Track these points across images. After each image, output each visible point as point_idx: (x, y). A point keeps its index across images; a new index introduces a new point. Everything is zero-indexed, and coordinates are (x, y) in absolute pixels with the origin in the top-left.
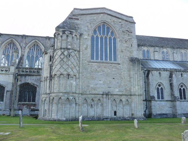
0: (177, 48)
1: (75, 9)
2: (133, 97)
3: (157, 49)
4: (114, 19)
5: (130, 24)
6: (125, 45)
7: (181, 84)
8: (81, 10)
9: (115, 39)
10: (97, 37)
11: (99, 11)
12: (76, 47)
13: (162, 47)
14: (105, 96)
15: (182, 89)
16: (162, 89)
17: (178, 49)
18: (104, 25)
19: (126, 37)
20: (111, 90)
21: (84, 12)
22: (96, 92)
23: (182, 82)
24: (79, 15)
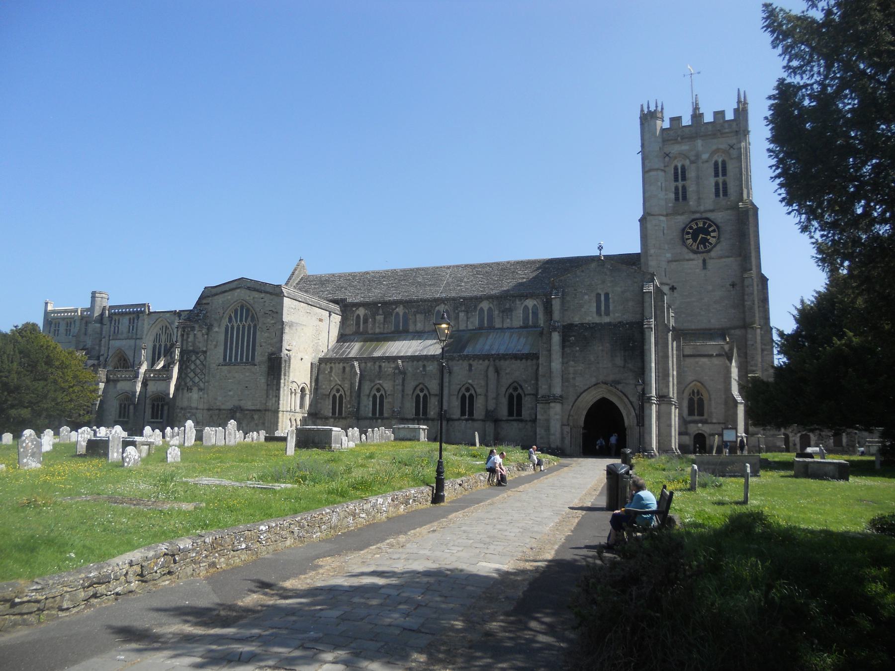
1: (206, 288)
4: (256, 295)
7: (421, 386)
9: (255, 326)
18: (242, 307)
19: (270, 321)
20: (242, 403)
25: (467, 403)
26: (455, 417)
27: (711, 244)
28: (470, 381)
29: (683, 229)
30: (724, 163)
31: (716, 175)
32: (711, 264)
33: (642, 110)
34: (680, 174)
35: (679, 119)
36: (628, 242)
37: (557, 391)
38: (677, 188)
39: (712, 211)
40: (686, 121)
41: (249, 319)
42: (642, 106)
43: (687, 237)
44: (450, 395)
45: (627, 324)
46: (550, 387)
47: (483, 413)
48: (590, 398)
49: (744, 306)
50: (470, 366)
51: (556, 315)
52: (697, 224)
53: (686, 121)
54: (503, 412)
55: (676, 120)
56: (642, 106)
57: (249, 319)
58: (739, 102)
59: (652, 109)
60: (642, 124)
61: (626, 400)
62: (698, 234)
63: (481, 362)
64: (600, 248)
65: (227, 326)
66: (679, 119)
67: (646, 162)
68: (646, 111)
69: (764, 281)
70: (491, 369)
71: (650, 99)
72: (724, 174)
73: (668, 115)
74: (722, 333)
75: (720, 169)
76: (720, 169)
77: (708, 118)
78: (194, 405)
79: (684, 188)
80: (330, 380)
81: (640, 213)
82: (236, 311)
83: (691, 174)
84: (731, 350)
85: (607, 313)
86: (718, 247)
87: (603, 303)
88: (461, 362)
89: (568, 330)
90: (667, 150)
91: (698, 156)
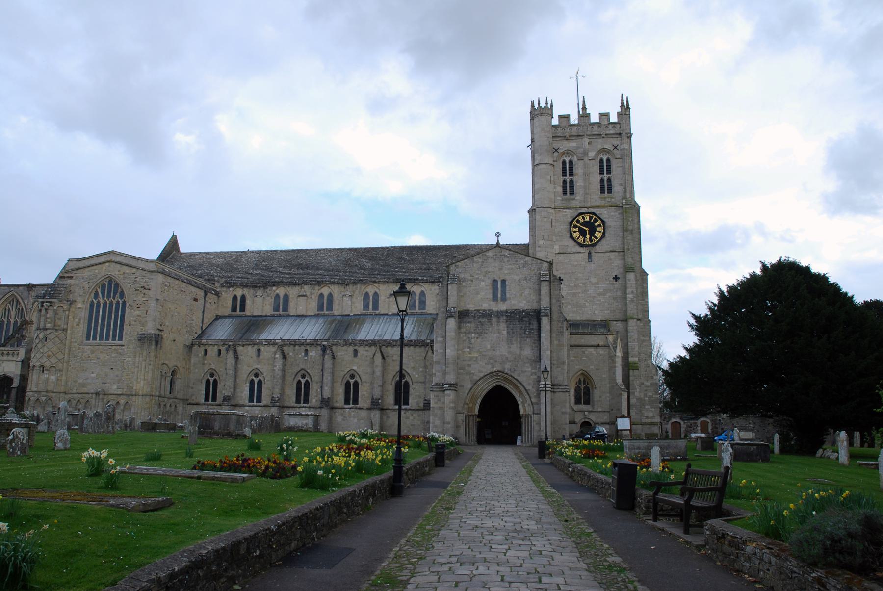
0: (355, 283)
1: (70, 260)
2: (134, 398)
3: (307, 289)
4: (127, 270)
5: (149, 275)
6: (137, 313)
7: (303, 372)
8: (78, 260)
9: (124, 303)
10: (99, 302)
11: (102, 259)
12: (61, 324)
13: (319, 283)
14: (94, 396)
15: (303, 381)
16: (260, 382)
17: (359, 286)
18: (110, 282)
19: (140, 299)
21: (81, 264)
22: (86, 390)
23: (302, 366)
24: (73, 270)
25: (352, 392)
26: (338, 405)
27: (596, 238)
28: (355, 368)
29: (571, 222)
30: (608, 160)
31: (602, 172)
32: (595, 257)
33: (533, 106)
34: (568, 169)
35: (567, 117)
36: (517, 232)
37: (451, 378)
38: (564, 182)
39: (598, 207)
40: (574, 119)
41: (118, 295)
42: (533, 102)
43: (574, 230)
44: (333, 382)
45: (524, 311)
46: (445, 373)
47: (369, 402)
48: (485, 387)
49: (626, 298)
50: (356, 352)
51: (452, 302)
52: (584, 218)
53: (574, 119)
54: (390, 399)
55: (565, 118)
56: (533, 102)
57: (118, 295)
58: (622, 106)
59: (543, 105)
60: (532, 119)
61: (522, 388)
62: (587, 228)
63: (367, 348)
64: (498, 235)
65: (92, 302)
66: (567, 117)
67: (536, 155)
68: (536, 106)
69: (644, 275)
70: (378, 356)
71: (541, 94)
72: (609, 172)
73: (557, 112)
74: (605, 325)
75: (605, 167)
76: (605, 167)
77: (595, 119)
78: (50, 388)
79: (572, 182)
80: (203, 364)
81: (529, 206)
82: (104, 285)
83: (579, 170)
84: (615, 342)
85: (504, 299)
86: (603, 241)
87: (499, 288)
88: (345, 347)
89: (463, 315)
90: (556, 145)
91: (585, 153)
